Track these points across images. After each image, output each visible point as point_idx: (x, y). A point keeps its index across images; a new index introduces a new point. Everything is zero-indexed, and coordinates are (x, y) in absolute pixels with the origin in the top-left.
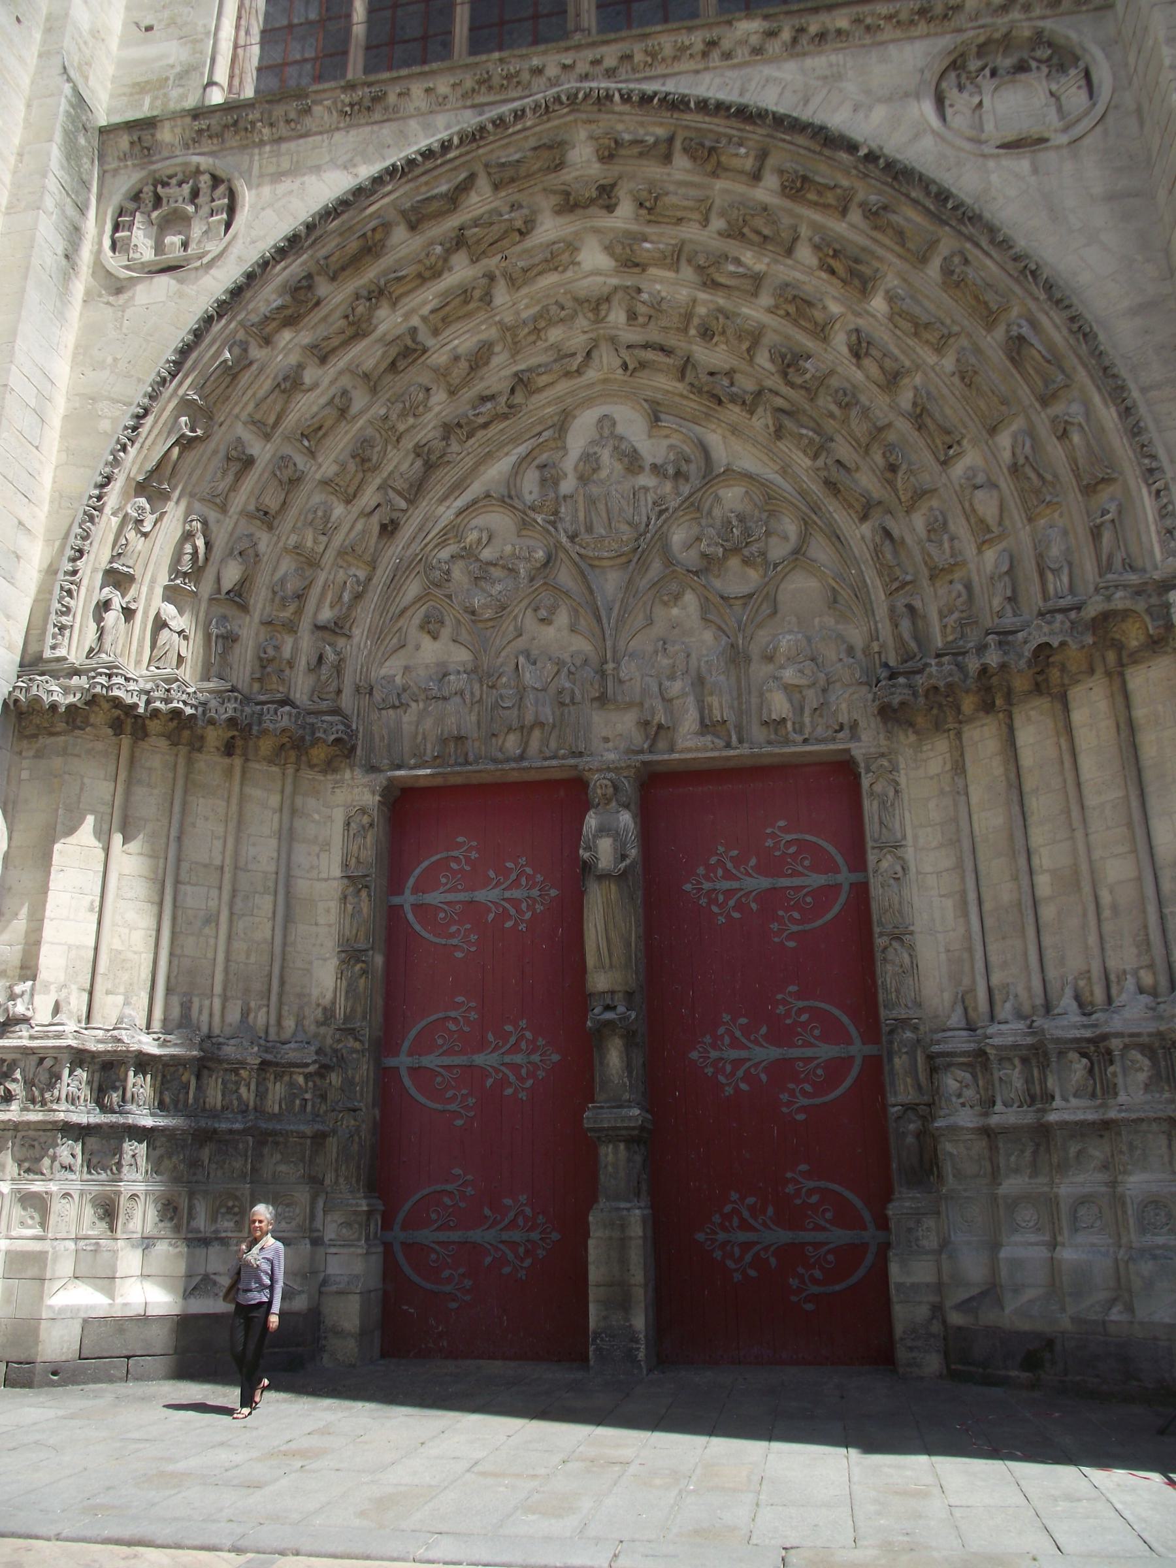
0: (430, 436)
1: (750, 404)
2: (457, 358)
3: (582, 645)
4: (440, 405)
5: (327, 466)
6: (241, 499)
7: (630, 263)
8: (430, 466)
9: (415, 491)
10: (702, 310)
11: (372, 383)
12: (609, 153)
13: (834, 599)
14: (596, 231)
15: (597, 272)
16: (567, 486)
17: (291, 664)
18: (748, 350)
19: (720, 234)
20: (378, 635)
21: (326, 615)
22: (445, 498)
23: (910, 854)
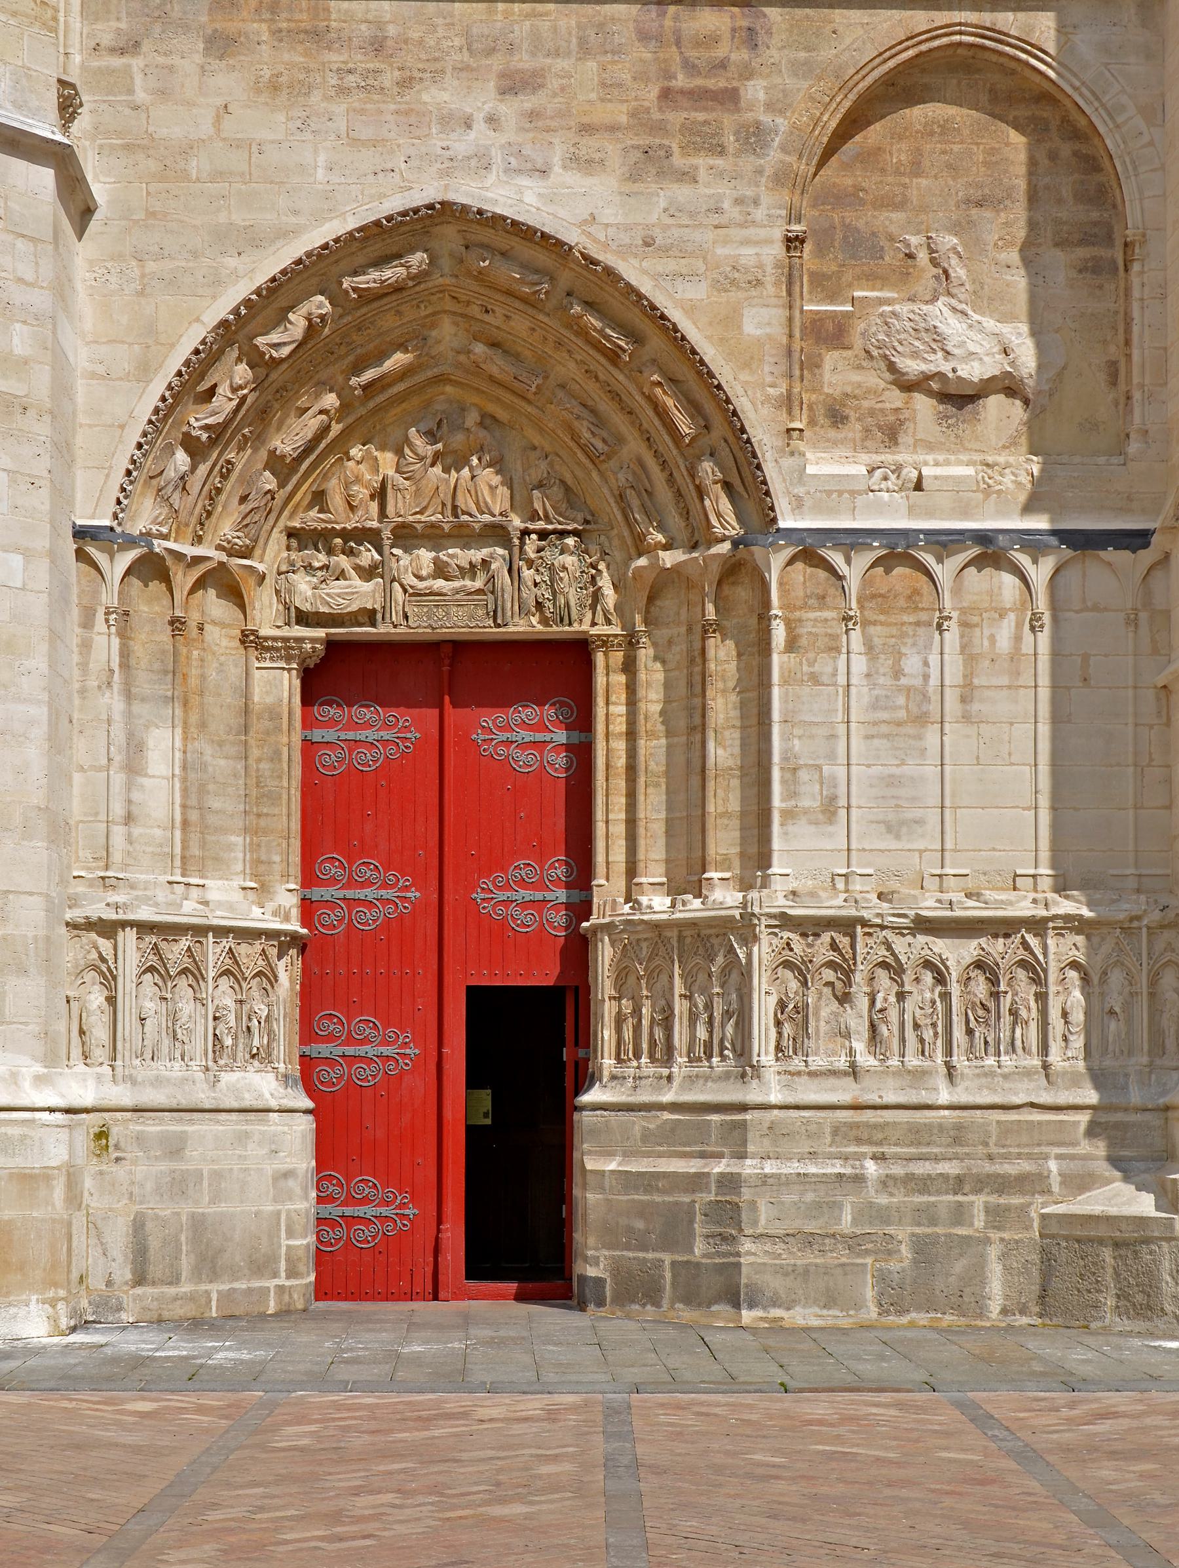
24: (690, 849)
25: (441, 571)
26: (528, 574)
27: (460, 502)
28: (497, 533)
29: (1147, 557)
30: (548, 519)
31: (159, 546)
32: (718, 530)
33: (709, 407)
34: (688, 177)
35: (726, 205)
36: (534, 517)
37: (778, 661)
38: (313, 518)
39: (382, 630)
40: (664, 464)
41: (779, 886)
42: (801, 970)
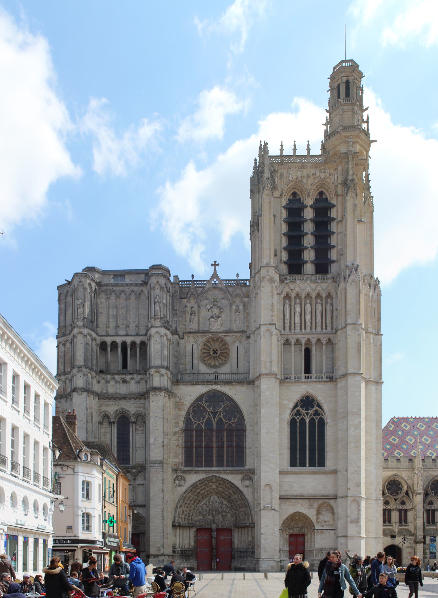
1: (226, 498)
3: (212, 518)
4: (201, 496)
5: (192, 502)
6: (186, 506)
7: (217, 487)
9: (198, 503)
11: (196, 496)
12: (216, 480)
16: (211, 503)
20: (195, 516)
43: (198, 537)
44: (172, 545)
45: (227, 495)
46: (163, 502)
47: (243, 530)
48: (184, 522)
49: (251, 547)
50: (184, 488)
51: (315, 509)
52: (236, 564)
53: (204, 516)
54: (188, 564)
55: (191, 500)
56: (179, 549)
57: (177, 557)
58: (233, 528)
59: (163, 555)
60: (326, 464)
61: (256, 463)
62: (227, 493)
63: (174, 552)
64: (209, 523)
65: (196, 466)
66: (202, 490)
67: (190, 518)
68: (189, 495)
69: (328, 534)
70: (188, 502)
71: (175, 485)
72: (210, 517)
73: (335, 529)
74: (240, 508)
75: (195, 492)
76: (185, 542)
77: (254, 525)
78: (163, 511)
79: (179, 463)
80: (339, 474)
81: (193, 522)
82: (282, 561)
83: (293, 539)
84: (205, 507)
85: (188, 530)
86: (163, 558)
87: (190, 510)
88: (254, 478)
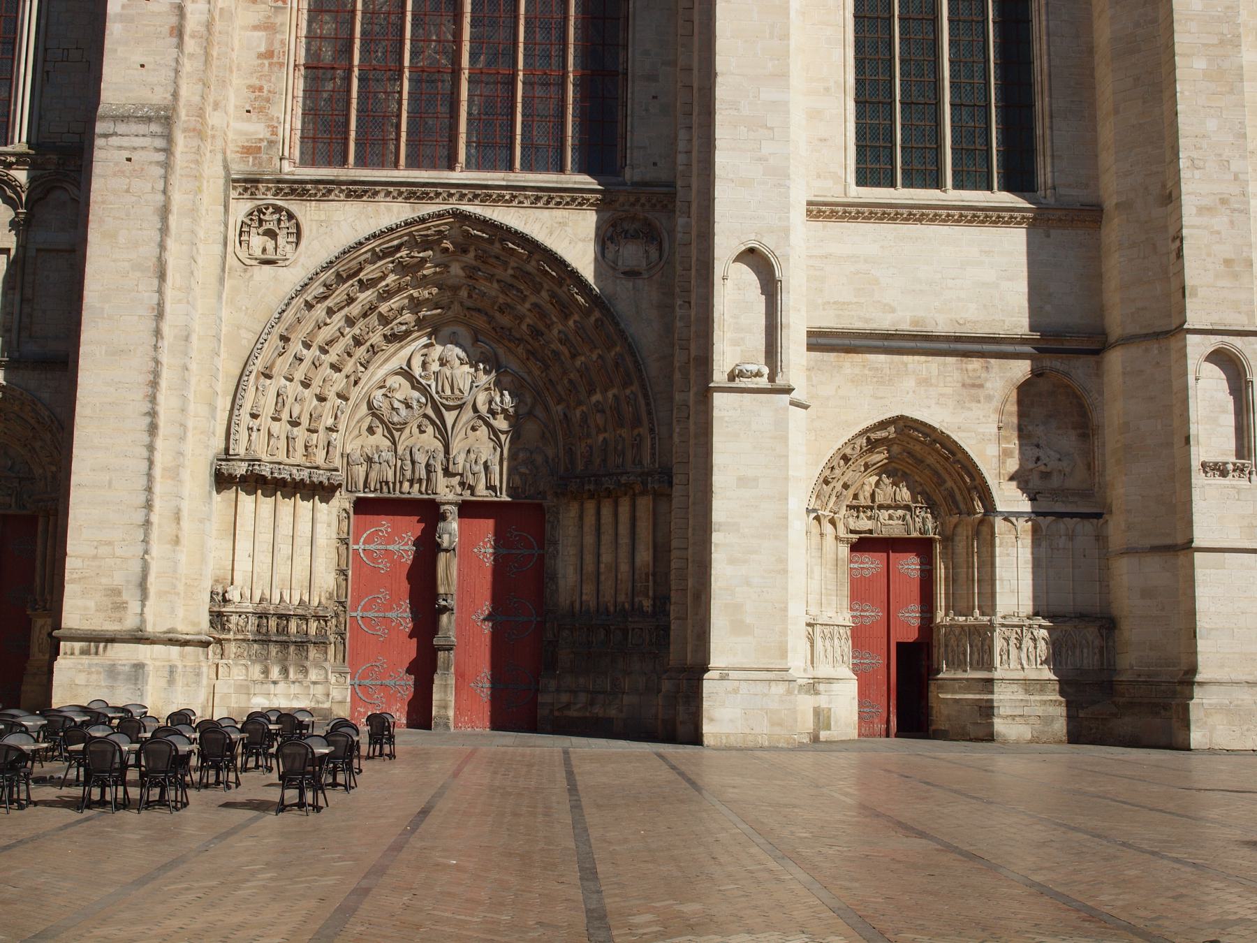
0: (378, 340)
2: (392, 309)
5: (332, 357)
6: (299, 375)
8: (375, 353)
10: (501, 301)
13: (543, 436)
14: (458, 261)
15: (457, 276)
16: (435, 367)
17: (316, 446)
18: (518, 324)
19: (511, 275)
21: (330, 422)
22: (381, 365)
23: (560, 548)
24: (968, 601)
25: (891, 518)
26: (917, 519)
27: (897, 498)
28: (907, 508)
29: (1101, 521)
30: (922, 503)
31: (820, 512)
32: (978, 511)
33: (974, 474)
34: (970, 409)
35: (981, 417)
36: (917, 502)
37: (998, 550)
38: (855, 503)
39: (875, 535)
40: (960, 489)
41: (999, 615)
42: (1007, 640)
43: (360, 547)
44: (207, 585)
45: (521, 318)
46: (158, 333)
47: (606, 512)
48: (282, 456)
49: (647, 604)
50: (291, 276)
51: (996, 403)
52: (565, 698)
53: (392, 429)
54: (295, 689)
55: (330, 343)
56: (248, 607)
57: (232, 648)
58: (548, 502)
59: (139, 637)
60: (1041, 179)
61: (681, 146)
62: (524, 308)
63: (218, 619)
64: (423, 475)
65: (361, 162)
66: (387, 295)
67: (322, 436)
68: (320, 311)
69: (1062, 542)
70: (309, 355)
71: (243, 254)
72: (430, 440)
73: (1098, 516)
74: (591, 392)
75: (351, 300)
76: (283, 570)
77: (671, 484)
78: (154, 384)
79: (271, 143)
80: (1114, 230)
81: (337, 462)
82: (821, 687)
83: (871, 563)
84: (404, 390)
85: (305, 506)
86: (143, 652)
87: (321, 399)
88: (672, 232)
